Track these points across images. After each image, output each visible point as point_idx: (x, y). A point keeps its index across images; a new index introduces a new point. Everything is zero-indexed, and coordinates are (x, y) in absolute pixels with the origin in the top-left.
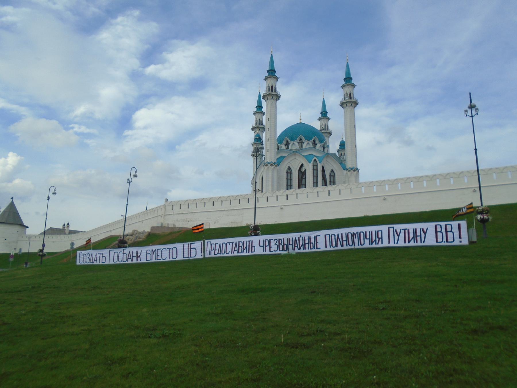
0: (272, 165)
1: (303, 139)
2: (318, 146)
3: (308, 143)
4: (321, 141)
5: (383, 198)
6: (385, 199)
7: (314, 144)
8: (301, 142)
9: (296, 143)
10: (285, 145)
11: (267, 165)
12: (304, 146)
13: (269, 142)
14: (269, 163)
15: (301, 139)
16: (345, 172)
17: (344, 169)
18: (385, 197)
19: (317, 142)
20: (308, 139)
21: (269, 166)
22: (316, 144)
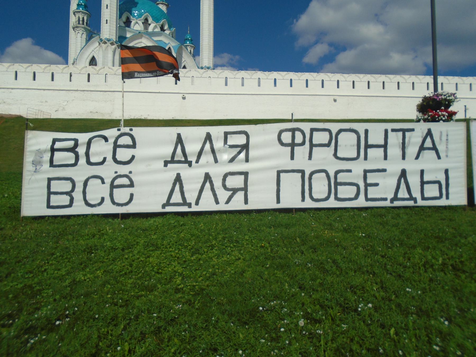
0: (112, 44)
1: (150, 20)
2: (167, 32)
3: (156, 27)
4: (170, 27)
5: (332, 98)
6: (335, 101)
7: (162, 29)
8: (146, 23)
9: (140, 23)
10: (124, 23)
11: (105, 43)
12: (150, 29)
13: (108, 10)
14: (109, 40)
15: (146, 20)
16: (201, 71)
17: (199, 68)
18: (335, 97)
19: (166, 27)
20: (156, 20)
21: (108, 44)
22: (164, 31)
